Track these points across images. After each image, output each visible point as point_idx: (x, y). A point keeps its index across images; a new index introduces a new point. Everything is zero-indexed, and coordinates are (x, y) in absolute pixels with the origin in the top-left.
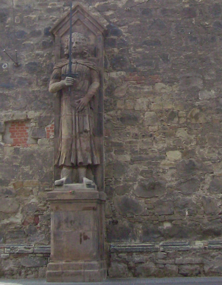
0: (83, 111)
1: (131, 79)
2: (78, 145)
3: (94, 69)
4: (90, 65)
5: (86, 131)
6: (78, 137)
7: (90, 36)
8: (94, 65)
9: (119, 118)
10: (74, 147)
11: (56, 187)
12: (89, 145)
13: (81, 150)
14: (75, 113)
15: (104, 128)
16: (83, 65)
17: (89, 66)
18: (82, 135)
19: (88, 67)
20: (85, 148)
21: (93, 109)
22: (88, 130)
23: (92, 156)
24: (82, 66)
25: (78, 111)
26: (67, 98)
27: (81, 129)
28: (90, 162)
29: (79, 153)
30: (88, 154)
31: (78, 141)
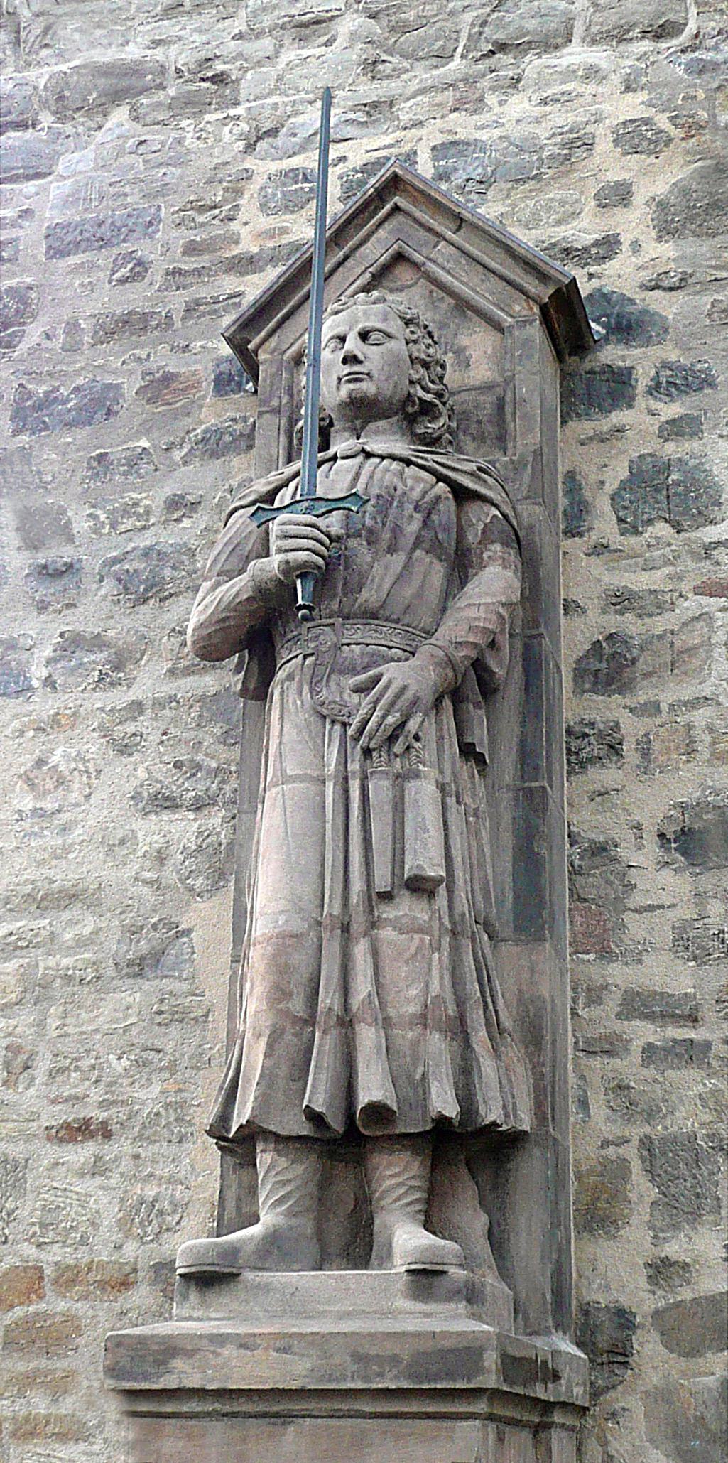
0: (398, 748)
2: (362, 987)
3: (483, 491)
4: (454, 469)
6: (358, 925)
7: (464, 341)
8: (480, 469)
9: (670, 836)
10: (328, 998)
11: (185, 1297)
12: (438, 984)
13: (387, 1023)
14: (344, 760)
16: (408, 462)
17: (450, 474)
18: (387, 912)
19: (440, 478)
20: (413, 1009)
21: (480, 759)
22: (435, 870)
24: (395, 466)
28: (444, 1102)
30: (438, 1046)
31: (361, 951)
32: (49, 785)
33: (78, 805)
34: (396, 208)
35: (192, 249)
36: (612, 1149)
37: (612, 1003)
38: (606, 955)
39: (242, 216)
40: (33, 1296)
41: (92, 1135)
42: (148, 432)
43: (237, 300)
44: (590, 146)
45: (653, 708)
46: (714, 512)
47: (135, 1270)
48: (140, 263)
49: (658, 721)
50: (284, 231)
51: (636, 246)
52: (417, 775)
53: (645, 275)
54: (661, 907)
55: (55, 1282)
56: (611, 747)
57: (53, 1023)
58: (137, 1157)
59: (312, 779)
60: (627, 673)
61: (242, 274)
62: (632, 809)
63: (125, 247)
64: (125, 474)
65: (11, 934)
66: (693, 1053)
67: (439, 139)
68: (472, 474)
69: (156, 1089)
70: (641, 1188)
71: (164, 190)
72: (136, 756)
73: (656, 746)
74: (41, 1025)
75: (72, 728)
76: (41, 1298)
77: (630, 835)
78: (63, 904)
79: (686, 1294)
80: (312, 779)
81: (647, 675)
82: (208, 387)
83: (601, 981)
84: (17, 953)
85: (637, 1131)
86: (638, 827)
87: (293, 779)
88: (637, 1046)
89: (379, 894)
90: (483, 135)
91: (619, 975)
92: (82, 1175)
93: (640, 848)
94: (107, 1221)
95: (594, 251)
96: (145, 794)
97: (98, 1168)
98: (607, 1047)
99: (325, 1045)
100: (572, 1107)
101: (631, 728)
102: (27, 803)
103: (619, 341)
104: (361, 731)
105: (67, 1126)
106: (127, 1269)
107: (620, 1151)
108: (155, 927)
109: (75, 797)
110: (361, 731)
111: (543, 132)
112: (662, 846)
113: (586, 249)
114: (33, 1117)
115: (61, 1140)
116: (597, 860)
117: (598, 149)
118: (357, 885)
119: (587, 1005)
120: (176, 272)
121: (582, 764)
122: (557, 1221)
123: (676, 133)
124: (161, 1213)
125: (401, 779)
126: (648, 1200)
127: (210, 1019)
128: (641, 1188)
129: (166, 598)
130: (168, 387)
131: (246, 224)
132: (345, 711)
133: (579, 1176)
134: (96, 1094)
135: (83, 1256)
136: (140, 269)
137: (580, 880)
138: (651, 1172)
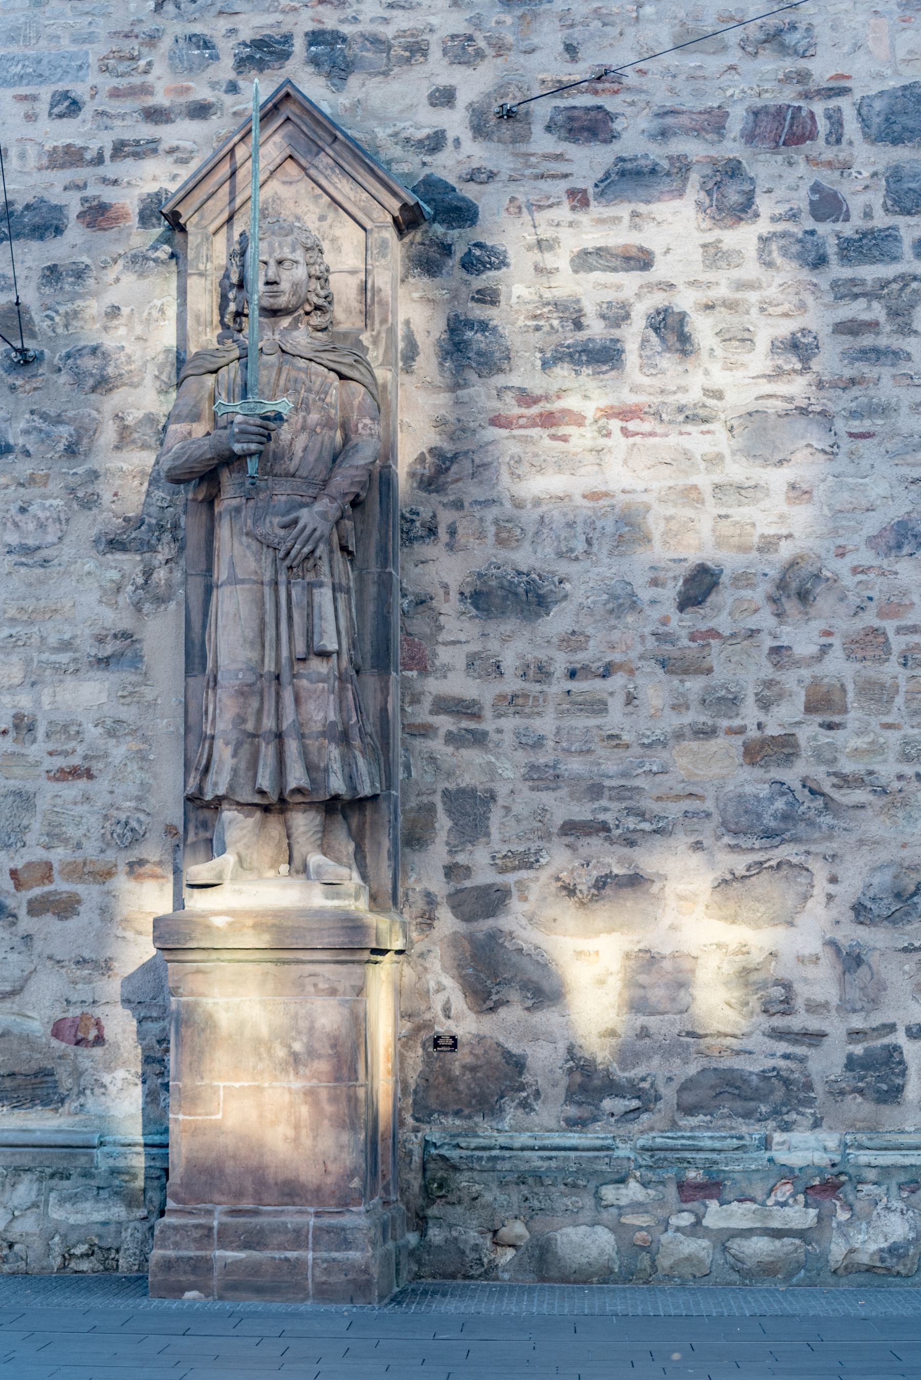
0: (310, 563)
1: (522, 421)
5: (324, 655)
6: (285, 677)
7: (338, 232)
9: (467, 594)
13: (302, 736)
15: (399, 636)
16: (311, 360)
21: (350, 553)
22: (332, 646)
23: (348, 764)
25: (287, 562)
26: (238, 510)
27: (300, 648)
29: (292, 746)
31: (288, 695)
32: (31, 526)
33: (54, 544)
34: (288, 119)
35: (116, 94)
36: (425, 797)
37: (427, 703)
38: (424, 671)
39: (157, 71)
40: (46, 881)
41: (80, 776)
42: (88, 251)
43: (152, 146)
44: (425, 53)
45: (458, 505)
46: (505, 366)
47: (116, 866)
48: (74, 102)
49: (462, 514)
50: (188, 89)
51: (457, 142)
52: (321, 585)
53: (464, 170)
54: (460, 642)
55: (60, 872)
56: (430, 530)
57: (46, 700)
58: (112, 792)
59: (255, 582)
60: (442, 479)
61: (156, 123)
62: (442, 574)
63: (61, 87)
64: (73, 284)
65: (11, 636)
66: (479, 739)
67: (310, 26)
68: (351, 366)
69: (123, 749)
70: (443, 822)
71: (90, 38)
72: (95, 511)
73: (460, 531)
74: (37, 702)
75: (45, 485)
76: (51, 882)
77: (441, 592)
78: (47, 616)
79: (468, 884)
80: (255, 582)
81: (457, 480)
82: (134, 220)
83: (420, 689)
84: (16, 649)
85: (442, 786)
86: (446, 587)
87: (243, 581)
88: (442, 732)
89: (299, 659)
90: (346, 29)
91: (434, 686)
92: (75, 803)
93: (447, 601)
94: (96, 833)
95: (427, 142)
96: (103, 539)
97: (87, 799)
98: (423, 732)
99: (268, 752)
100: (401, 769)
101: (445, 517)
102: (12, 538)
103: (441, 222)
104: (288, 554)
105: (61, 770)
106: (110, 865)
107: (430, 798)
108: (115, 636)
109: (51, 538)
110: (288, 553)
111: (388, 32)
112: (461, 601)
113: (420, 141)
114: (37, 764)
115: (58, 780)
116: (421, 608)
117: (431, 58)
118: (285, 653)
119: (412, 703)
120: (103, 113)
121: (411, 540)
122: (395, 844)
123: (490, 52)
124: (132, 830)
125: (311, 586)
126: (446, 828)
127: (159, 701)
128: (443, 822)
129: (110, 390)
130: (103, 215)
131: (159, 78)
132: (276, 540)
133: (404, 812)
134: (81, 750)
135: (79, 856)
136: (74, 107)
137: (408, 622)
138: (449, 812)
